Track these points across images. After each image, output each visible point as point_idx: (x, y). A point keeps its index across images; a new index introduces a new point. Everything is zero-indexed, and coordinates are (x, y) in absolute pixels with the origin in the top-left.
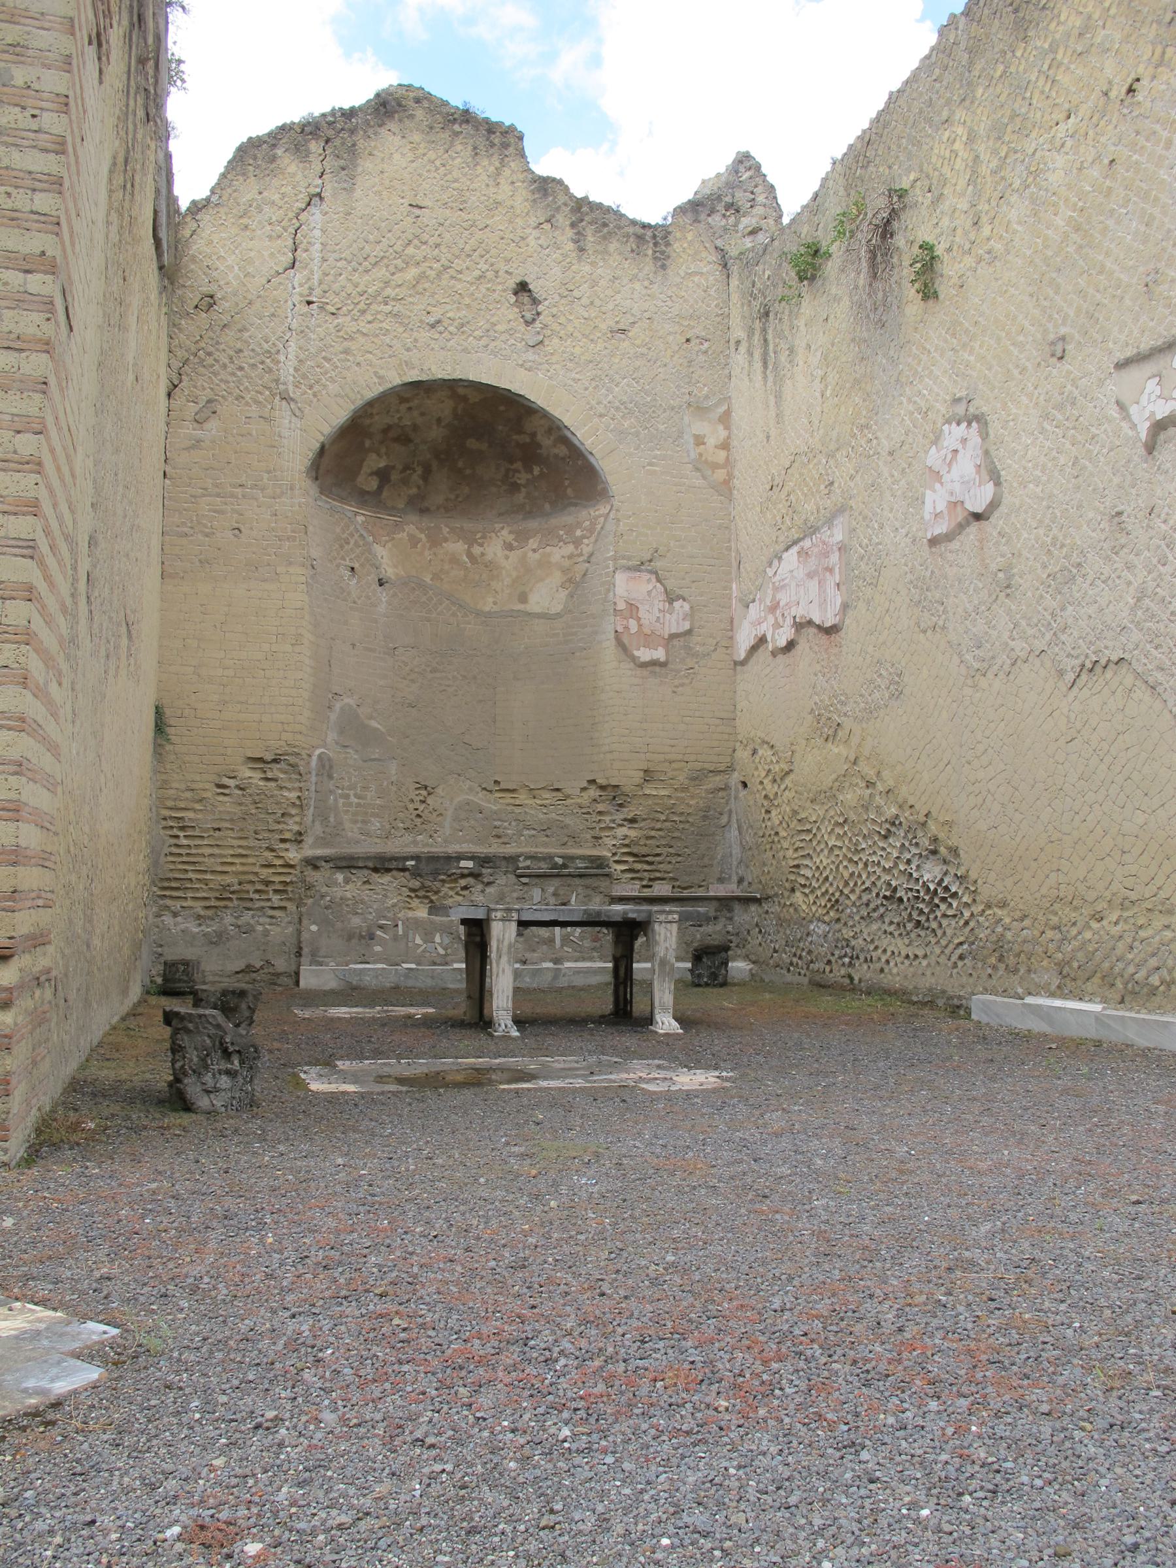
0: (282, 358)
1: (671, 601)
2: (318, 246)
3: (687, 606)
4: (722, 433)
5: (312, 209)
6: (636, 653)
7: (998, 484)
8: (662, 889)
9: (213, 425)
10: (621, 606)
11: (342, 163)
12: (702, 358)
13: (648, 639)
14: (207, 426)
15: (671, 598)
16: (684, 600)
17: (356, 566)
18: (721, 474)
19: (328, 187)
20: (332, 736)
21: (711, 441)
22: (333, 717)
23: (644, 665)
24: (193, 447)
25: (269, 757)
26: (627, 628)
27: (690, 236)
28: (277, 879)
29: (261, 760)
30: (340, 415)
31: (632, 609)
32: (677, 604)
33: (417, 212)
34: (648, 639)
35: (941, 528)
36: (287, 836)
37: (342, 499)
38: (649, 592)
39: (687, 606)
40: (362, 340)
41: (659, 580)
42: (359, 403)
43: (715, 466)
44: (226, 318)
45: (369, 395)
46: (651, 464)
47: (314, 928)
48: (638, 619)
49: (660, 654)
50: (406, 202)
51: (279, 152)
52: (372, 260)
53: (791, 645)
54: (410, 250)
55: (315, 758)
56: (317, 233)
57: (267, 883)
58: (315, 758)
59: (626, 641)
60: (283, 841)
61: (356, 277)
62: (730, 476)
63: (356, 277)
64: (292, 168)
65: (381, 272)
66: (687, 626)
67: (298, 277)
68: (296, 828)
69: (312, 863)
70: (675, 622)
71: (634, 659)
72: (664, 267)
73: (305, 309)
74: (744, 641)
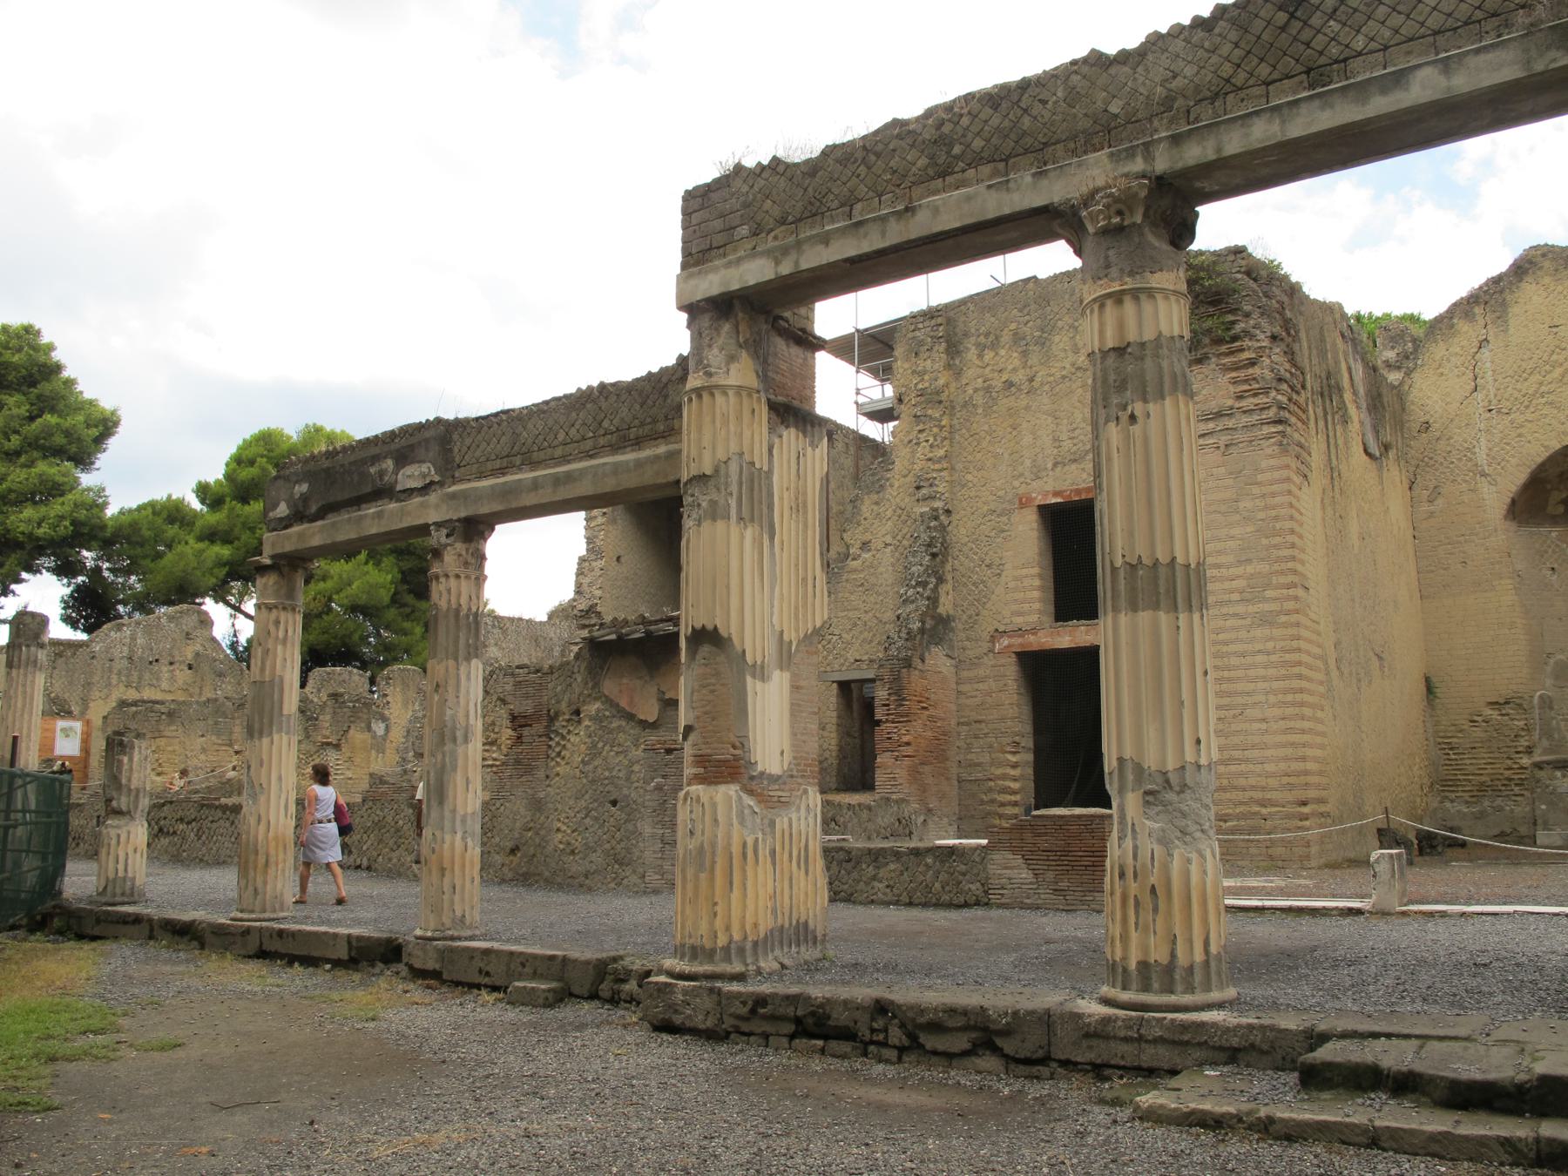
0: (1477, 450)
2: (1490, 373)
5: (1483, 350)
9: (1440, 502)
11: (1498, 314)
14: (1436, 503)
17: (1556, 566)
19: (1491, 333)
20: (1549, 682)
22: (1549, 669)
24: (1429, 517)
25: (1502, 701)
28: (1516, 777)
29: (1497, 703)
30: (1521, 477)
33: (1555, 330)
36: (1520, 749)
37: (1539, 525)
40: (1529, 425)
42: (1534, 466)
44: (1438, 434)
45: (1539, 460)
47: (1543, 807)
50: (1546, 326)
51: (1455, 321)
52: (1528, 371)
54: (1555, 357)
55: (1536, 698)
56: (1488, 365)
57: (1510, 780)
58: (1536, 698)
60: (1517, 752)
61: (1519, 386)
63: (1519, 386)
64: (1466, 328)
65: (1534, 379)
67: (1479, 396)
68: (1527, 744)
69: (1539, 766)
73: (1489, 415)
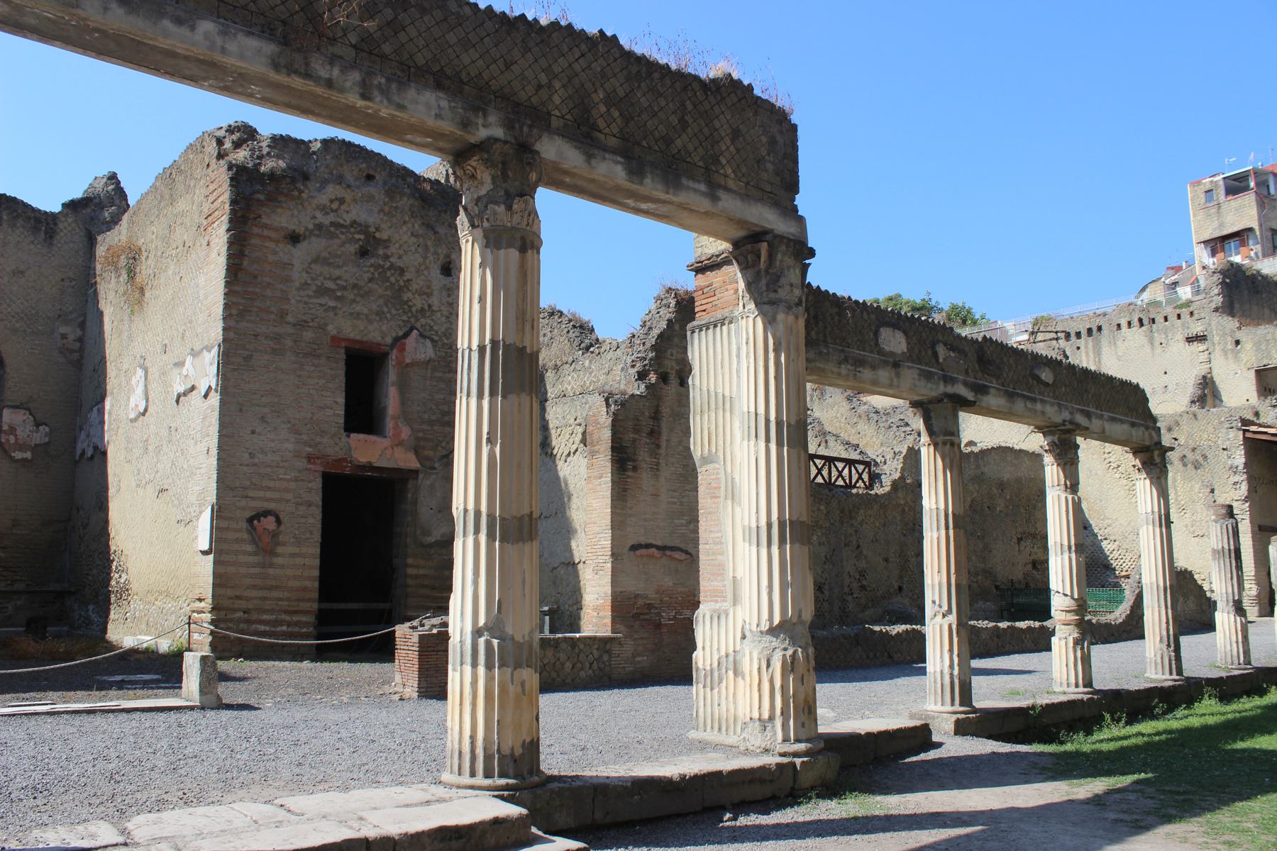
1: (38, 425)
3: (47, 429)
4: (79, 332)
6: (13, 454)
7: (147, 401)
8: (20, 586)
10: (5, 427)
12: (70, 290)
13: (21, 447)
15: (38, 425)
16: (46, 425)
18: (75, 356)
21: (71, 337)
23: (18, 461)
26: (8, 440)
27: (70, 220)
31: (12, 430)
32: (41, 428)
34: (21, 447)
35: (132, 416)
38: (24, 421)
39: (47, 429)
41: (31, 414)
43: (73, 351)
46: (31, 349)
48: (16, 436)
49: (28, 455)
53: (92, 457)
59: (7, 447)
62: (82, 357)
66: (47, 440)
70: (40, 436)
71: (12, 458)
72: (51, 237)
74: (79, 452)
